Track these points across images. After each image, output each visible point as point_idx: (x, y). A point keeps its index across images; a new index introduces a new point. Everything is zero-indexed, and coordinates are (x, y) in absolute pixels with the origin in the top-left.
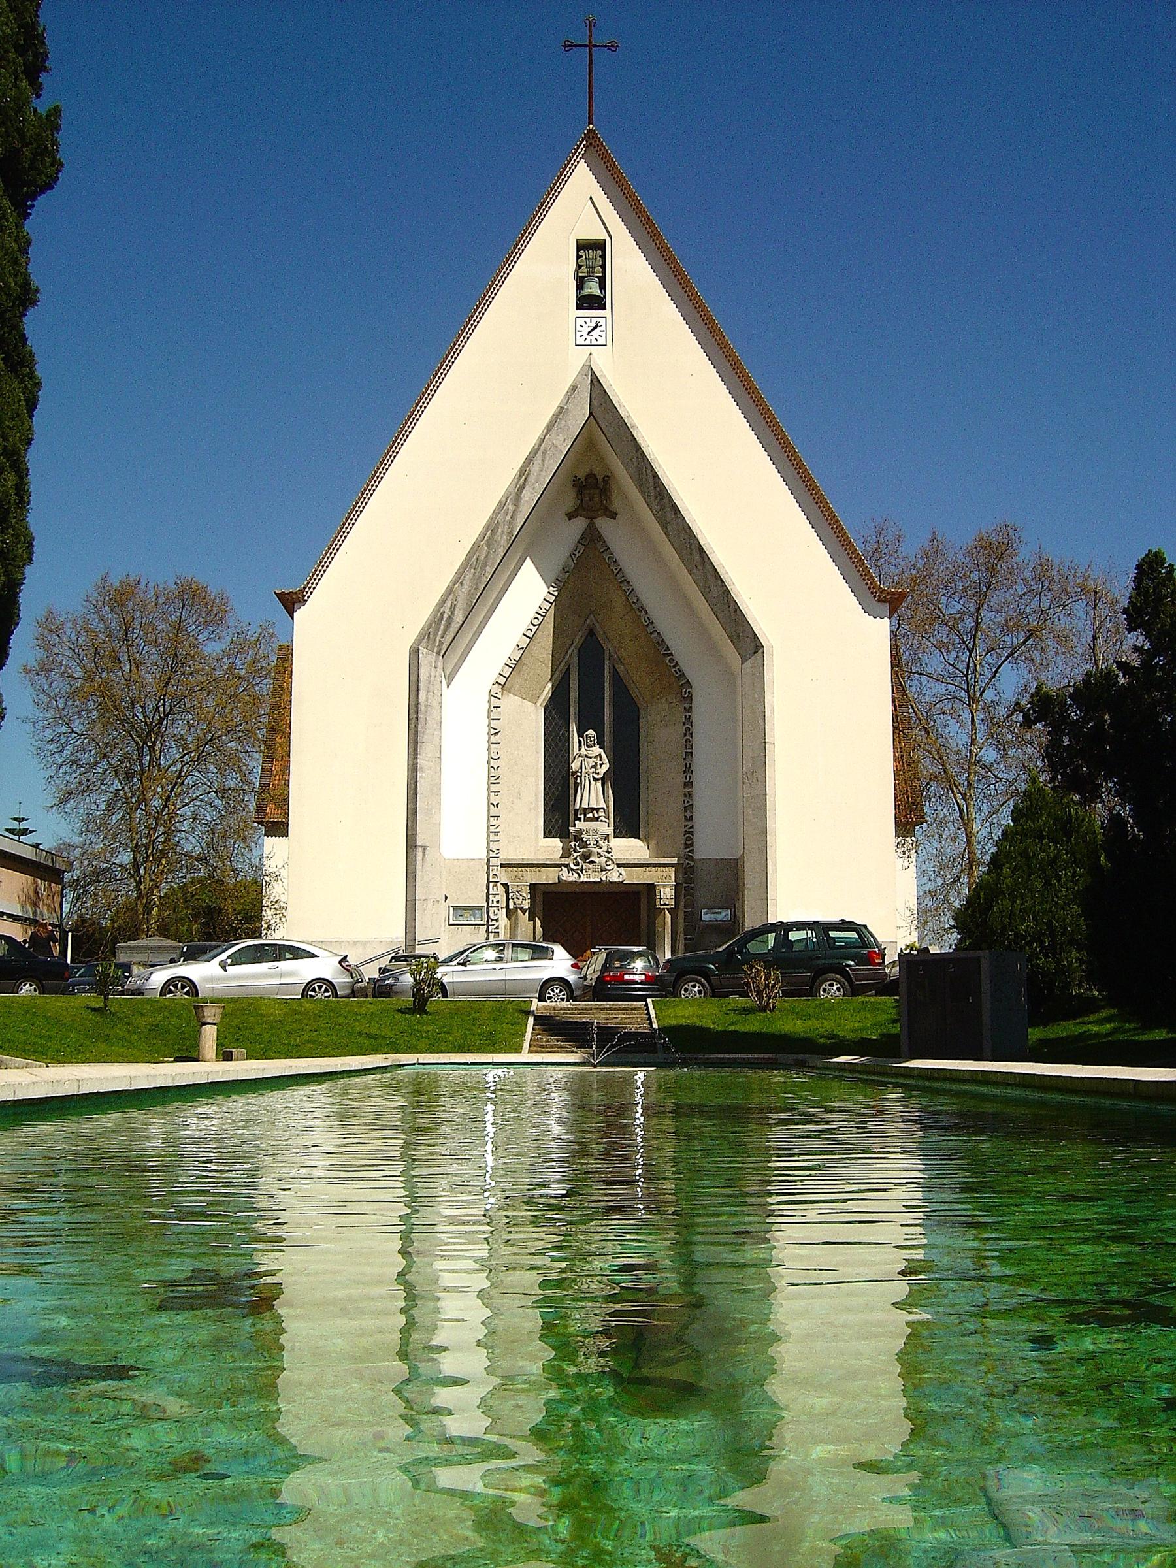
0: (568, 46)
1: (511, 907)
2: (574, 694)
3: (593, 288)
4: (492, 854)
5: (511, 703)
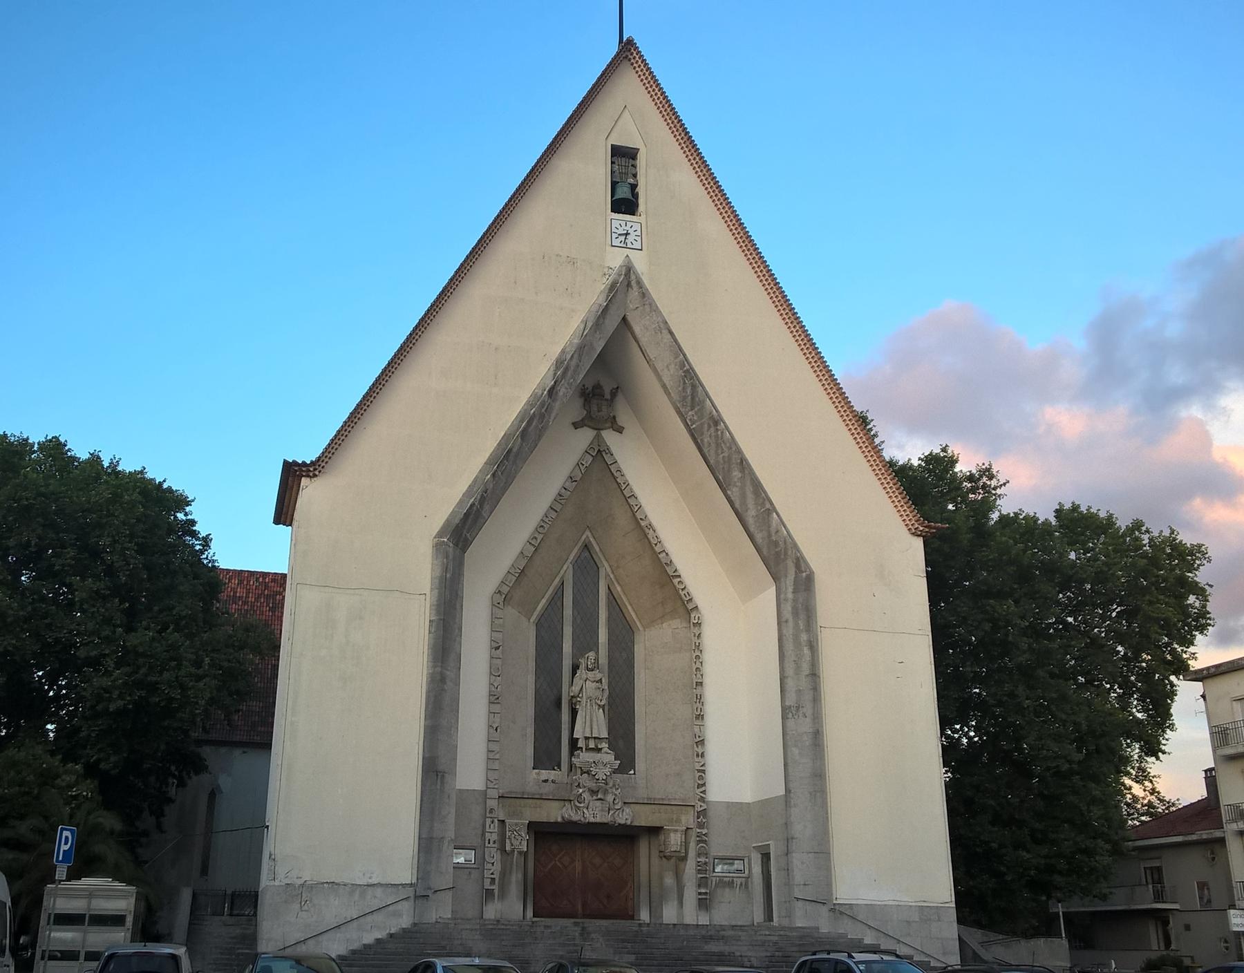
1: (508, 848)
2: (568, 612)
5: (511, 612)
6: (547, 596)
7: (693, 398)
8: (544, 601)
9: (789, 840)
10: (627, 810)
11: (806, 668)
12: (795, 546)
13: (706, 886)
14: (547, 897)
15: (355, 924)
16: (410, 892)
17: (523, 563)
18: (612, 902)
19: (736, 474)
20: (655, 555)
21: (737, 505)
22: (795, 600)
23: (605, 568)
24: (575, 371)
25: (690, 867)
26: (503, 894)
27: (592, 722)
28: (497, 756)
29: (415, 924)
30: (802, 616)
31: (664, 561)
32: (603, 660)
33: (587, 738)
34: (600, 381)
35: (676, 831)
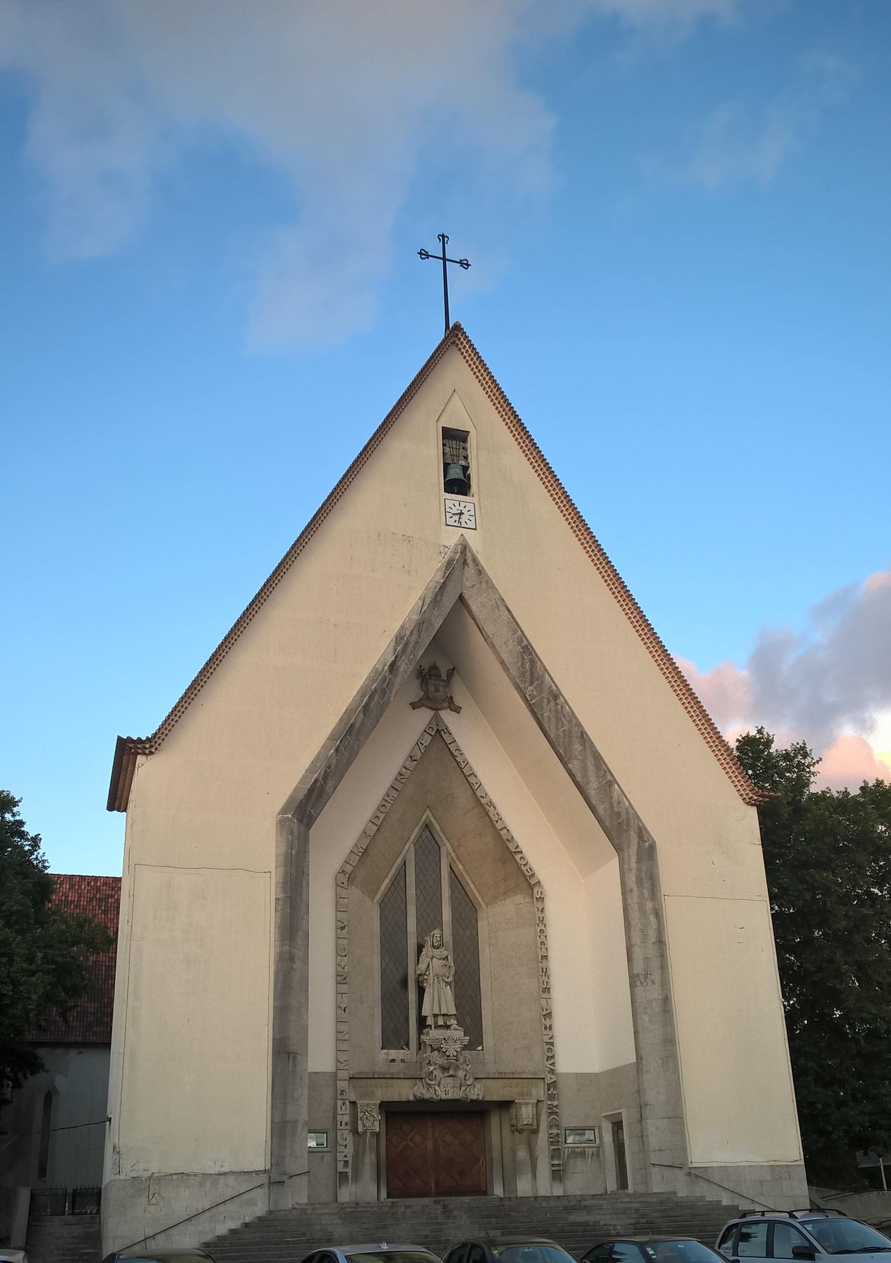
1: (360, 1129)
2: (411, 891)
4: (340, 1066)
5: (355, 893)
6: (390, 876)
7: (532, 675)
8: (387, 881)
9: (642, 1107)
10: (478, 1085)
11: (652, 936)
13: (559, 1158)
14: (400, 1177)
15: (208, 1214)
16: (264, 1179)
17: (365, 843)
18: (464, 1178)
19: (577, 747)
20: (496, 833)
21: (579, 779)
22: (639, 870)
23: (447, 847)
24: (414, 647)
25: (542, 1140)
26: (357, 1176)
27: (440, 999)
28: (346, 1037)
29: (271, 1212)
30: (647, 885)
31: (505, 837)
32: (448, 938)
33: (435, 1016)
34: (435, 663)
35: (527, 1104)
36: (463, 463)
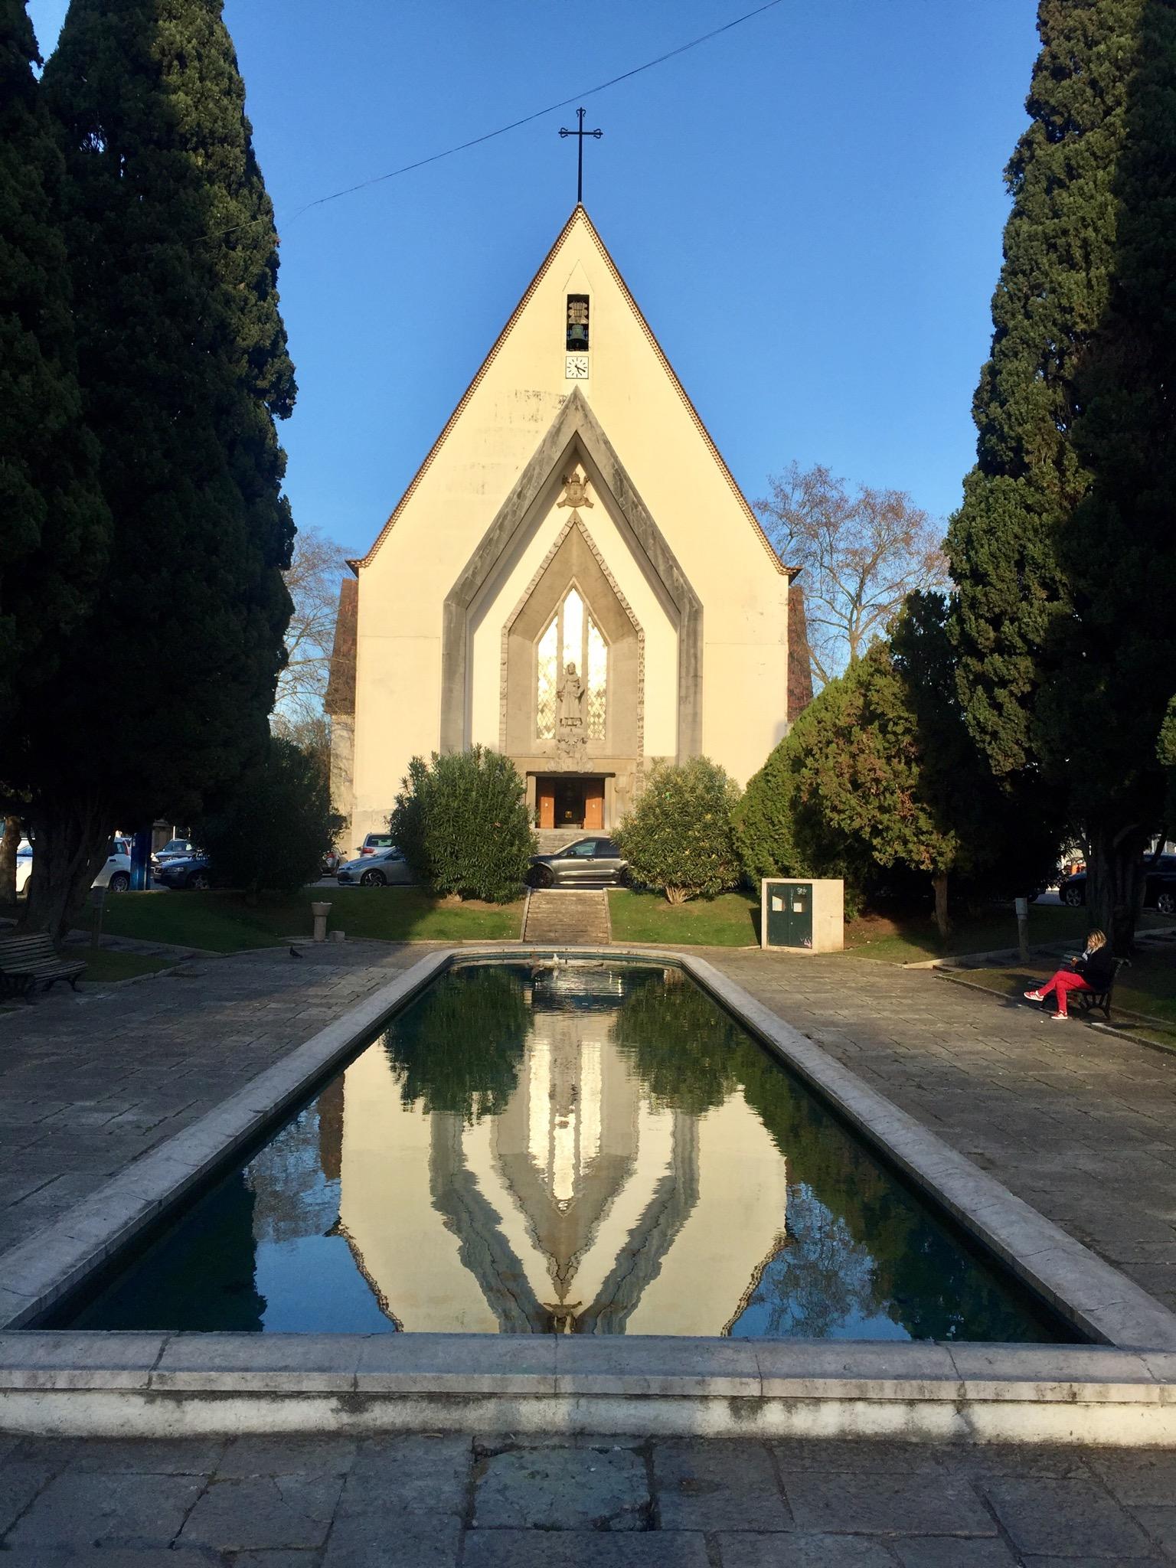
0: (564, 133)
3: (578, 333)
5: (516, 639)
12: (691, 590)
36: (584, 321)
